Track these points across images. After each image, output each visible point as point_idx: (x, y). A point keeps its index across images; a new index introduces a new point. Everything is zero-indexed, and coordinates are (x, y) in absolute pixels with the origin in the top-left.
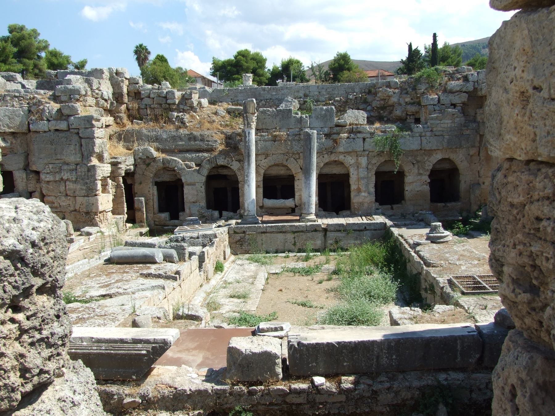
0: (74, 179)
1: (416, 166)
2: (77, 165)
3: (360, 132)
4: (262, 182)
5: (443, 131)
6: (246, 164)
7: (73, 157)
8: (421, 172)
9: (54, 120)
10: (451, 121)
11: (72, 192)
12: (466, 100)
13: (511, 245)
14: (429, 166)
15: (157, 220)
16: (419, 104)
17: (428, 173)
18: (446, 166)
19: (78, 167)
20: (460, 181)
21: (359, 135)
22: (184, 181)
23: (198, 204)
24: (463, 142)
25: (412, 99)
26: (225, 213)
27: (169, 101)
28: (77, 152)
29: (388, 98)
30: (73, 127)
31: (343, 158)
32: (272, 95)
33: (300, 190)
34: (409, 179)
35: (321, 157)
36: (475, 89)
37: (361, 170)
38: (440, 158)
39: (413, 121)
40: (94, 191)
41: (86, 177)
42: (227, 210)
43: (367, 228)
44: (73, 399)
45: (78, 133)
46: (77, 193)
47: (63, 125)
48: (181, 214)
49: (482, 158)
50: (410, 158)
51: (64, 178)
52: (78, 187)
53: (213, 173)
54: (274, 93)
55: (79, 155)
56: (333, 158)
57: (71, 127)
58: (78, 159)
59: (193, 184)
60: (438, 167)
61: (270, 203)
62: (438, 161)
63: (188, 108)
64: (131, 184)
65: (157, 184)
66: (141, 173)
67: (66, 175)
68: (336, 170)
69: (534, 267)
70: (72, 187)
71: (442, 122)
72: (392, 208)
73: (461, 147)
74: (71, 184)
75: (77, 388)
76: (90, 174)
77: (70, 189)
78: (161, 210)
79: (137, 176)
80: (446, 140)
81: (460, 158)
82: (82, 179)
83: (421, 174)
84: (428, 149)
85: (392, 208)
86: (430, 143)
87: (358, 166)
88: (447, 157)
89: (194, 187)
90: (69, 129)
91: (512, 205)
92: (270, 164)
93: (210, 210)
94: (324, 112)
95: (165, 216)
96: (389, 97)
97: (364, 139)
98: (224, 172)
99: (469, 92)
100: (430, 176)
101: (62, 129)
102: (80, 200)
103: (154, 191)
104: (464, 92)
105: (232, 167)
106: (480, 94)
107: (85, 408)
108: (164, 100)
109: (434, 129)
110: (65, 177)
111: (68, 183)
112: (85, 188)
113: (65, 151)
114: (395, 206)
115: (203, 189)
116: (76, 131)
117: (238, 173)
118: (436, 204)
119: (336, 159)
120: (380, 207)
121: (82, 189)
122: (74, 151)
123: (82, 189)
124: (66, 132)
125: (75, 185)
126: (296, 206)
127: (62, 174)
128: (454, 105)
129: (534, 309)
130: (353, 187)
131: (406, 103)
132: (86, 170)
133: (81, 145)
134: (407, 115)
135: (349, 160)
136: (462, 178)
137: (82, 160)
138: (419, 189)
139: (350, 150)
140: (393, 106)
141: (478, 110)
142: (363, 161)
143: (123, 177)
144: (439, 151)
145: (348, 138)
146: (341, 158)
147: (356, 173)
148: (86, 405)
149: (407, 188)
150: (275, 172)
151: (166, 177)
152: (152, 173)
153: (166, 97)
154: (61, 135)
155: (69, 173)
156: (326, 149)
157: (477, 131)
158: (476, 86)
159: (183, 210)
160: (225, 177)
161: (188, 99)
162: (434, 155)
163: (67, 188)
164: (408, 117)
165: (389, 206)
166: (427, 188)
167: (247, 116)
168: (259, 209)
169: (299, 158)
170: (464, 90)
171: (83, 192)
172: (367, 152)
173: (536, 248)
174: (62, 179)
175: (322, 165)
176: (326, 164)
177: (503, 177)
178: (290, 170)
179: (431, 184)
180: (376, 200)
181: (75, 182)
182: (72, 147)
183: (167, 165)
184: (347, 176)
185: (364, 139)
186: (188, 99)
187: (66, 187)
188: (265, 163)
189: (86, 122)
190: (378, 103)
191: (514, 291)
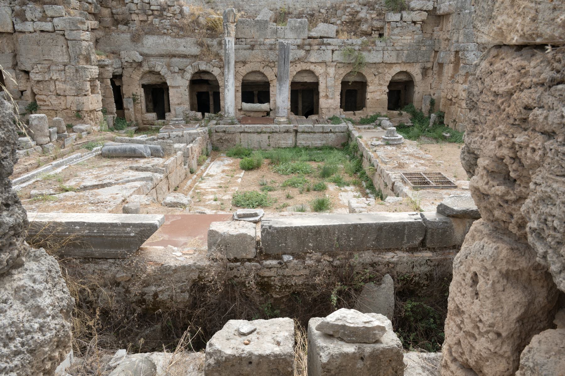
1: (377, 77)
2: (65, 65)
3: (329, 44)
4: (241, 88)
5: (403, 46)
6: (226, 70)
7: (60, 58)
8: (381, 83)
9: (39, 21)
10: (410, 37)
11: (62, 91)
12: (426, 19)
13: (490, 137)
14: (388, 78)
16: (384, 20)
17: (388, 84)
18: (403, 78)
19: (67, 68)
20: (414, 92)
21: (329, 47)
22: (168, 84)
23: (182, 106)
24: (420, 57)
25: (377, 16)
26: (206, 114)
27: (152, 8)
29: (356, 13)
30: (59, 28)
31: (314, 68)
32: (250, 6)
33: (275, 95)
34: (370, 88)
35: (294, 66)
36: (435, 8)
37: (329, 79)
38: (399, 71)
39: (377, 36)
42: (209, 112)
43: (332, 130)
44: (33, 287)
45: (64, 35)
47: (48, 26)
49: (435, 72)
50: (373, 70)
52: (68, 87)
53: (196, 78)
54: (252, 4)
55: (67, 57)
56: (305, 67)
57: (56, 29)
58: (66, 61)
59: (178, 87)
60: (397, 78)
61: (247, 106)
62: (397, 74)
63: (171, 15)
64: (120, 86)
65: (143, 86)
66: (128, 76)
68: (308, 79)
69: (515, 158)
71: (403, 38)
72: (354, 114)
73: (417, 62)
74: (61, 84)
75: (38, 276)
77: (60, 89)
78: (148, 111)
79: (124, 78)
80: (404, 55)
81: (415, 71)
82: (71, 80)
83: (381, 85)
84: (388, 62)
85: (354, 114)
86: (390, 57)
87: (327, 74)
88: (405, 70)
89: (179, 90)
91: (496, 94)
92: (248, 72)
93: (194, 112)
94: (297, 25)
95: (152, 116)
96: (358, 12)
97: (333, 51)
98: (206, 77)
99: (429, 11)
100: (389, 87)
102: (70, 99)
103: (141, 92)
104: (424, 11)
105: (213, 73)
106: (438, 13)
107: (48, 296)
109: (396, 45)
110: (54, 78)
111: (57, 83)
112: (74, 88)
113: (52, 52)
114: (357, 112)
115: (187, 93)
117: (217, 77)
118: (392, 112)
119: (308, 69)
120: (345, 112)
122: (61, 53)
124: (51, 34)
125: (64, 85)
126: (271, 110)
127: (51, 75)
128: (415, 23)
129: (507, 202)
130: (322, 94)
131: (372, 18)
133: (68, 47)
134: (372, 30)
135: (319, 70)
136: (416, 89)
138: (378, 98)
139: (320, 60)
140: (359, 21)
141: (435, 28)
142: (332, 71)
143: (111, 80)
144: (398, 65)
145: (319, 49)
146: (312, 67)
147: (324, 81)
148: (49, 293)
149: (369, 96)
150: (252, 78)
153: (149, 3)
154: (47, 35)
155: (58, 74)
156: (298, 59)
157: (432, 48)
158: (436, 6)
159: (169, 111)
160: (207, 82)
162: (394, 68)
163: (57, 87)
164: (373, 32)
165: (352, 112)
166: (385, 97)
167: (227, 25)
168: (238, 111)
169: (274, 67)
170: (425, 8)
171: (73, 92)
172: (335, 63)
173: (520, 138)
174: (51, 78)
175: (295, 73)
176: (299, 73)
177: (488, 65)
178: (266, 77)
179: (390, 94)
180: (341, 107)
182: (59, 48)
183: (153, 69)
184: (317, 84)
185: (333, 51)
188: (244, 70)
189: (71, 24)
190: (347, 17)
191: (487, 183)
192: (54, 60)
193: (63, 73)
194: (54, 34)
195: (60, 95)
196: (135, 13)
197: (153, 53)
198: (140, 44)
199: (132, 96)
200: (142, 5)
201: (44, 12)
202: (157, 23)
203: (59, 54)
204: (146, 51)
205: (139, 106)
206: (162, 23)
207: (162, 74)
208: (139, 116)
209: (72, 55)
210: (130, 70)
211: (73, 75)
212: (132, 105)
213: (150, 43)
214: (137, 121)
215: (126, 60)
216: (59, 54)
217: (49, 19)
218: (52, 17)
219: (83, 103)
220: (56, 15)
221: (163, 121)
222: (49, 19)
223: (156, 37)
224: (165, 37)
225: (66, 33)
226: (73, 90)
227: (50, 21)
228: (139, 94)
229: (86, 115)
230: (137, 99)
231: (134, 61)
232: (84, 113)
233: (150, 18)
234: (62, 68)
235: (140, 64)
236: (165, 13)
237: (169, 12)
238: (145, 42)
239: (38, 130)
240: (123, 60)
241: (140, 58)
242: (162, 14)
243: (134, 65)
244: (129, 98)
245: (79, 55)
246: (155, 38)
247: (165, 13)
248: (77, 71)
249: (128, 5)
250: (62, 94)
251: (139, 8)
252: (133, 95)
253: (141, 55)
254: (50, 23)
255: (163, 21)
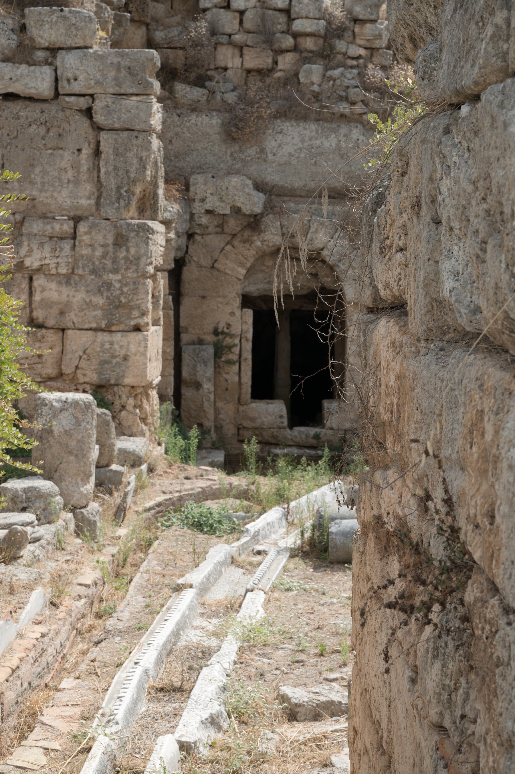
0: (63, 270)
2: (77, 220)
7: (65, 193)
11: (55, 311)
15: (247, 423)
19: (82, 228)
27: (298, 25)
28: (84, 177)
30: (76, 87)
40: (135, 313)
41: (108, 263)
45: (88, 112)
46: (72, 317)
47: (37, 81)
48: (326, 404)
51: (28, 262)
52: (79, 297)
55: (88, 188)
57: (64, 87)
58: (84, 202)
63: (362, 52)
65: (247, 301)
66: (206, 262)
67: (37, 255)
70: (54, 295)
74: (53, 285)
76: (122, 254)
77: (47, 304)
82: (94, 272)
90: (57, 94)
101: (32, 92)
102: (78, 341)
108: (282, 18)
110: (32, 262)
111: (39, 281)
112: (100, 301)
113: (38, 170)
116: (83, 103)
121: (89, 305)
123: (89, 305)
124: (45, 106)
125: (66, 291)
127: (23, 251)
132: (110, 240)
133: (97, 153)
137: (98, 204)
151: (284, 281)
152: (242, 265)
153: (287, 11)
154: (27, 112)
155: (47, 248)
161: (363, 22)
163: (37, 297)
171: (95, 317)
174: (20, 266)
181: (67, 279)
182: (66, 159)
186: (363, 22)
187: (31, 294)
189: (124, 73)
192: (42, 197)
193: (67, 246)
194: (53, 108)
195: (40, 326)
196: (230, 43)
197: (298, 184)
198: (252, 151)
199: (210, 338)
200: (263, 18)
201: (23, 28)
202: (316, 78)
203: (64, 178)
204: (273, 177)
205: (231, 375)
206: (330, 78)
207: (331, 260)
208: (228, 410)
209: (111, 183)
210: (215, 241)
211: (104, 256)
212: (210, 372)
213: (287, 149)
214: (218, 428)
215: (208, 206)
216: (64, 178)
217: (40, 55)
218: (54, 50)
219: (126, 358)
220: (70, 42)
221: (312, 431)
222: (40, 55)
223: (313, 126)
224: (344, 130)
225: (98, 106)
226: (95, 307)
227: (47, 63)
228: (236, 329)
229: (131, 401)
230: (230, 348)
231: (237, 211)
232: (123, 392)
233: (286, 62)
234: (67, 227)
235: (254, 223)
236: (341, 45)
237: (353, 42)
238: (271, 144)
239: (70, 453)
240: (197, 204)
241: (254, 203)
242: (332, 48)
243: (233, 225)
244: (201, 342)
245: (134, 182)
246: (311, 129)
247: (341, 45)
248: (120, 241)
249: (209, 15)
250: (51, 322)
251: (247, 25)
252: (216, 332)
253: (259, 187)
254: (47, 70)
255: (337, 72)
